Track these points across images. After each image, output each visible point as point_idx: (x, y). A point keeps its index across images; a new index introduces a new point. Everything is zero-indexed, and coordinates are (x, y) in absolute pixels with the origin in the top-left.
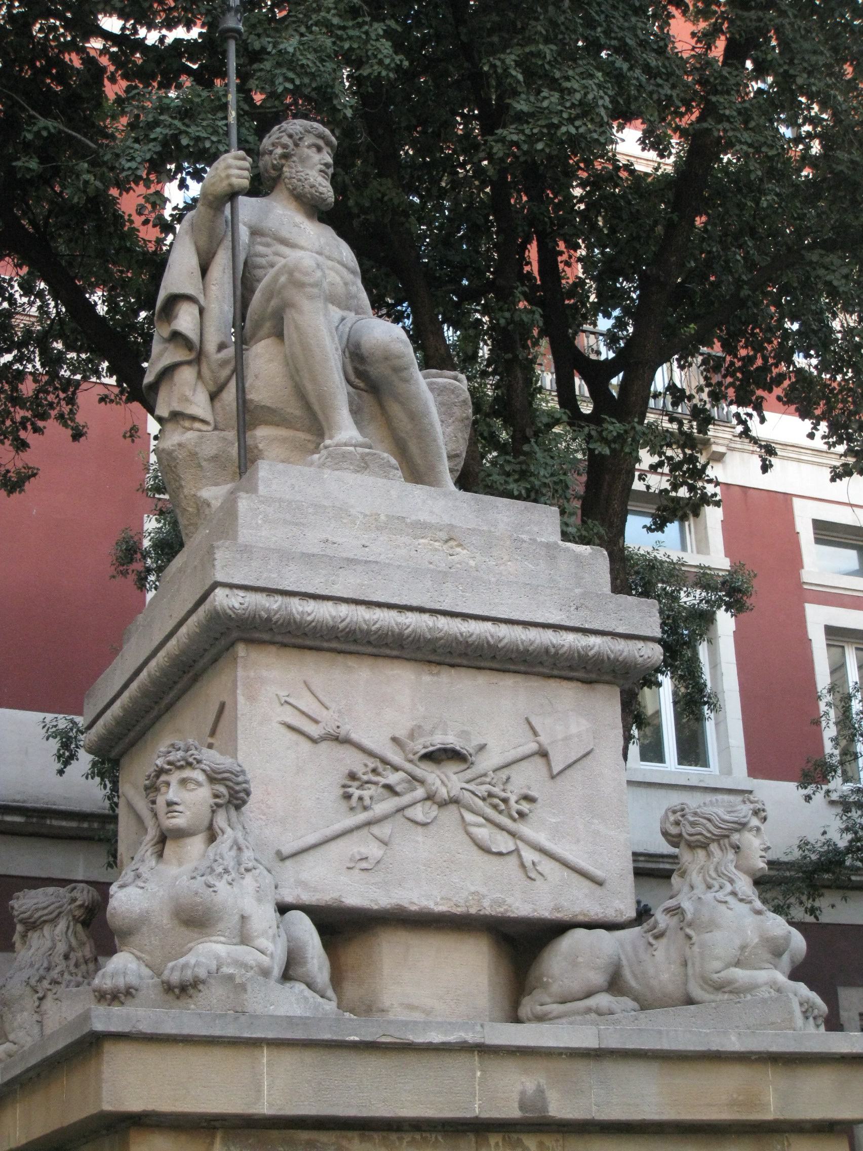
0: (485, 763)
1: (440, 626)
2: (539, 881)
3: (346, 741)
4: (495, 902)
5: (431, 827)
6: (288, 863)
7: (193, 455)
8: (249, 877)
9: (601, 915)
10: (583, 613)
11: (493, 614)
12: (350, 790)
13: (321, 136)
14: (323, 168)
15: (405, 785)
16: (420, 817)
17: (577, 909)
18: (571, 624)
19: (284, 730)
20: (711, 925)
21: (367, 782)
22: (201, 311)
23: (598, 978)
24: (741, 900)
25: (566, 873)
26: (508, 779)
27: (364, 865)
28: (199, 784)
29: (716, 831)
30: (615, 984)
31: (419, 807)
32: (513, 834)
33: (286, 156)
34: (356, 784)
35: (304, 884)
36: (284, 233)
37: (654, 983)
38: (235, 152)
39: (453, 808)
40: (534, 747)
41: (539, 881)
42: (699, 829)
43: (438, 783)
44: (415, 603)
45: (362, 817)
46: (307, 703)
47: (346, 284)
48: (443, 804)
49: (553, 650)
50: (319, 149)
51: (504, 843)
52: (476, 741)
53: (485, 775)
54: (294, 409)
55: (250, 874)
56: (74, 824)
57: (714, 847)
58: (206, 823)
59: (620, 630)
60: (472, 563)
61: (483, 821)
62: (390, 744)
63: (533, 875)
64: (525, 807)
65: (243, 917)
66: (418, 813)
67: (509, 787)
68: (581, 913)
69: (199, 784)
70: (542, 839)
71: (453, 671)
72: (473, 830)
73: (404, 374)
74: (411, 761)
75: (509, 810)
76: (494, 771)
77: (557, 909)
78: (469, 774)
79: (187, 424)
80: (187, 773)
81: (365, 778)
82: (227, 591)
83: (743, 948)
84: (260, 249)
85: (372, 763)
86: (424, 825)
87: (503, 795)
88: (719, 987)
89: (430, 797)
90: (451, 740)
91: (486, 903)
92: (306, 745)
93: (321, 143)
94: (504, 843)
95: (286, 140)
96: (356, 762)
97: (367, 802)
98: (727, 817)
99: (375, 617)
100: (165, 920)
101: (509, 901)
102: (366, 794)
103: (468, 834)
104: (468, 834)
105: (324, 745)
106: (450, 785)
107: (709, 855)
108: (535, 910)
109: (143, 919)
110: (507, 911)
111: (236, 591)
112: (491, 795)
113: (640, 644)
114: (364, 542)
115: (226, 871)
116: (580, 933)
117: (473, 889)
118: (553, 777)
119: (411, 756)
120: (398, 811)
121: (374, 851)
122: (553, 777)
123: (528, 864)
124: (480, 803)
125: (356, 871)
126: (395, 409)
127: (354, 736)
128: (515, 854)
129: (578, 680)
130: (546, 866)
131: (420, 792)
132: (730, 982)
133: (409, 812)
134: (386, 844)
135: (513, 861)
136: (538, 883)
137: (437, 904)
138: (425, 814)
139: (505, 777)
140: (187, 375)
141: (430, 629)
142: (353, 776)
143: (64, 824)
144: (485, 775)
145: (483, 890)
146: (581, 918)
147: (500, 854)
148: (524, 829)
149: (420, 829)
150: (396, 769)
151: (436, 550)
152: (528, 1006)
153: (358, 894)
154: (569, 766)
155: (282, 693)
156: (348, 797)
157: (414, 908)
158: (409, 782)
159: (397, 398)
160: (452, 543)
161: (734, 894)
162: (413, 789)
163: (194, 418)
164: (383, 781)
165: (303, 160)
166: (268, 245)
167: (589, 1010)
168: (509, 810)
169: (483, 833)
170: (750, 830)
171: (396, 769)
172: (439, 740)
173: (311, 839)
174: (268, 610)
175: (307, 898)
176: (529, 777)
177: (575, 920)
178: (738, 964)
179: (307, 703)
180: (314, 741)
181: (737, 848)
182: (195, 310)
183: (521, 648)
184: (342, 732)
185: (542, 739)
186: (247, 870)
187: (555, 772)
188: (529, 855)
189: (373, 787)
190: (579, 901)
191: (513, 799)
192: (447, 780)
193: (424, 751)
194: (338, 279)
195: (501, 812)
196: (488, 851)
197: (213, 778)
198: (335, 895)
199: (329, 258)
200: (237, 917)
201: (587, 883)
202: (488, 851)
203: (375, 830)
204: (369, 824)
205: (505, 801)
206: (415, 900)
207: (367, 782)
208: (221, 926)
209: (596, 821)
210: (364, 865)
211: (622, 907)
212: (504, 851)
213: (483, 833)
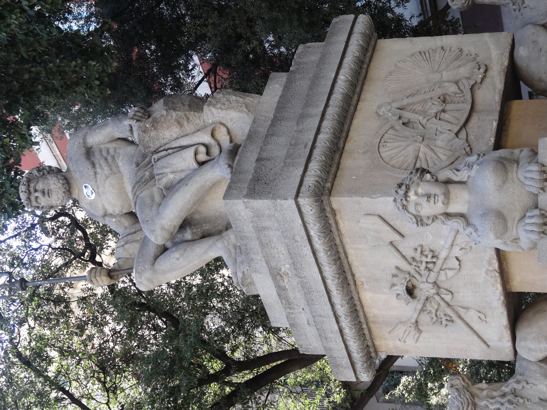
4: (490, 263)
10: (297, 238)
15: (433, 304)
27: (483, 317)
47: (107, 177)
48: (439, 287)
49: (329, 253)
50: (37, 198)
92: (424, 335)
93: (33, 198)
117: (484, 274)
125: (487, 320)
145: (483, 270)
148: (443, 255)
149: (454, 295)
157: (502, 298)
174: (363, 365)
188: (456, 252)
194: (108, 183)
198: (503, 328)
206: (498, 298)
210: (483, 317)
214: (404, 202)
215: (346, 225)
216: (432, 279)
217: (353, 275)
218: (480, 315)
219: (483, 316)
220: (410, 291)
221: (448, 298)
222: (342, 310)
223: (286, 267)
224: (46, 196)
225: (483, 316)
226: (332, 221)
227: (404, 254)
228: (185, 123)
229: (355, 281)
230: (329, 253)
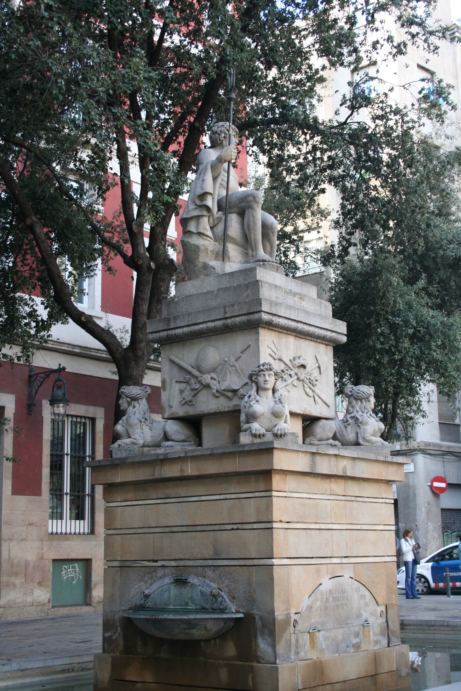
7: (206, 249)
19: (268, 355)
20: (367, 423)
23: (331, 435)
30: (335, 438)
37: (347, 438)
51: (311, 394)
79: (205, 237)
83: (374, 431)
88: (368, 441)
91: (307, 411)
94: (311, 394)
107: (362, 402)
112: (310, 379)
116: (324, 421)
132: (371, 440)
140: (206, 219)
152: (308, 440)
163: (207, 236)
164: (289, 373)
167: (328, 444)
169: (308, 390)
180: (275, 359)
213: (308, 390)
216: (306, 380)
217: (301, 338)
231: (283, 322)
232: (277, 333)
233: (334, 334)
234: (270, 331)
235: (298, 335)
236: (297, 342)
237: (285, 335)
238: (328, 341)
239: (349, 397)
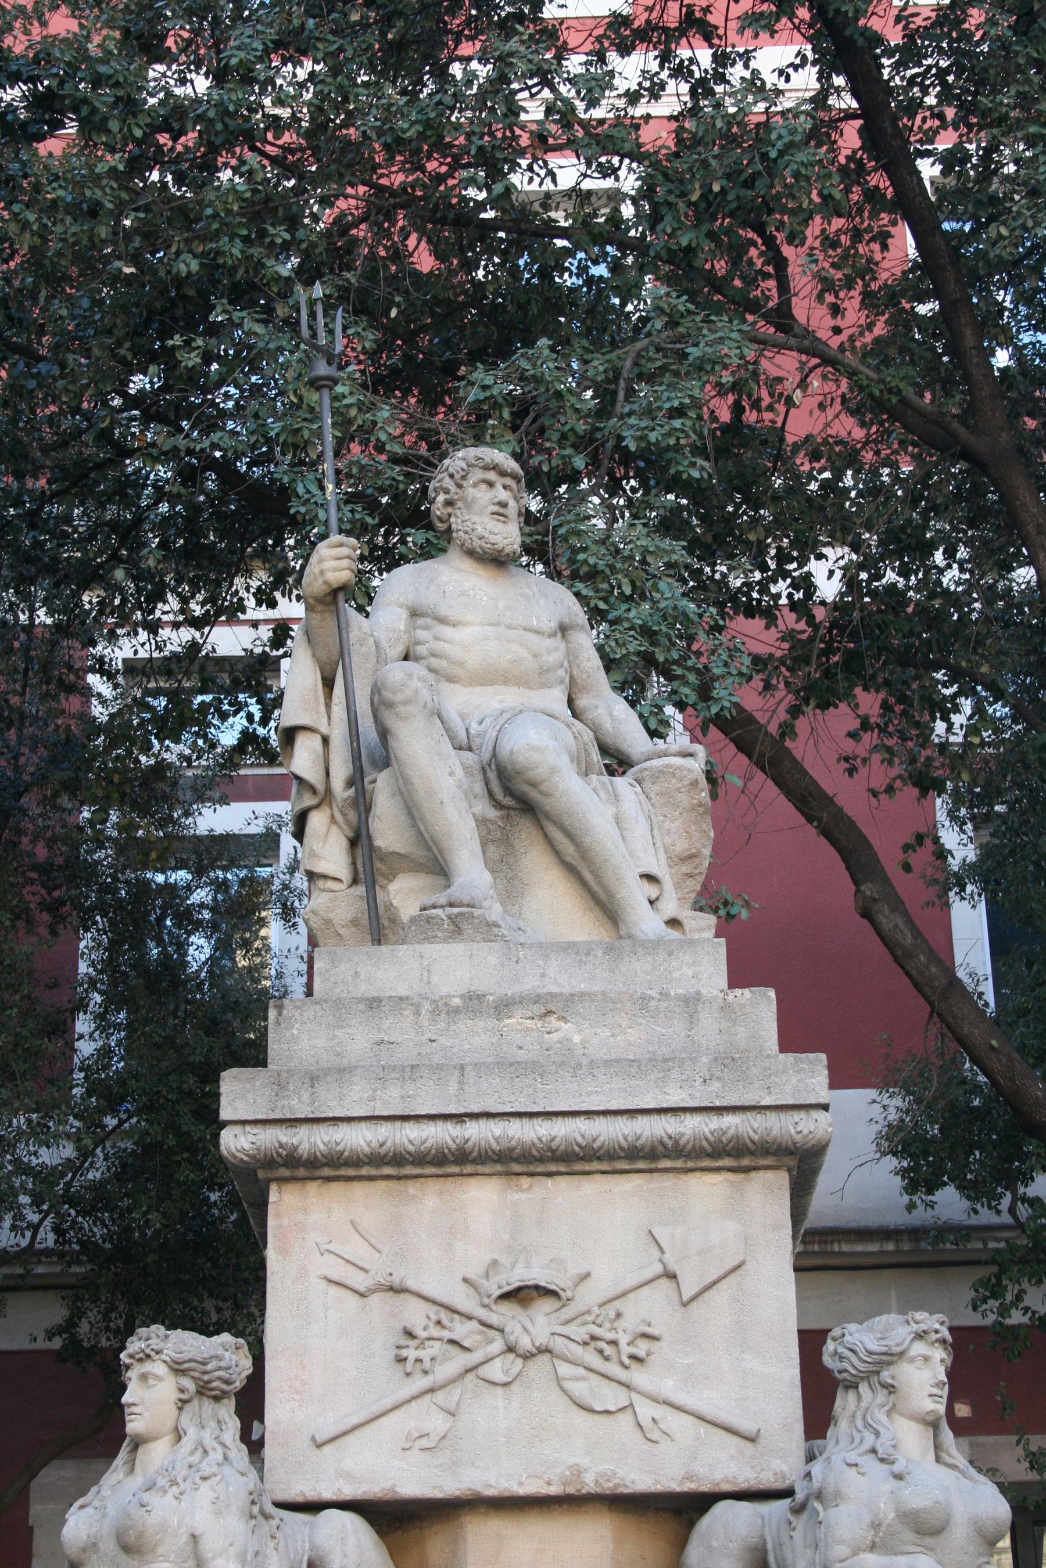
0: (588, 1297)
1: (511, 1133)
2: (664, 1444)
3: (396, 1290)
5: (514, 1387)
6: (326, 1449)
7: (328, 922)
8: (205, 1487)
9: (753, 1482)
10: (716, 1086)
11: (585, 1107)
12: (404, 1353)
13: (495, 467)
14: (496, 508)
16: (499, 1377)
17: (718, 1476)
18: (696, 1104)
19: (324, 1284)
21: (429, 1339)
22: (326, 740)
24: (882, 1460)
25: (703, 1429)
26: (619, 1315)
27: (425, 1443)
28: (159, 1378)
29: (862, 1367)
31: (497, 1363)
32: (628, 1386)
33: (449, 503)
34: (413, 1343)
35: (347, 1475)
36: (443, 611)
38: (335, 538)
39: (546, 1357)
40: (658, 1269)
41: (664, 1444)
42: (845, 1365)
43: (519, 1329)
44: (476, 1109)
45: (425, 1382)
46: (356, 1248)
48: (527, 1356)
50: (491, 484)
52: (575, 1269)
53: (588, 1312)
54: (420, 853)
55: (207, 1483)
56: (873, 1247)
57: (864, 1388)
58: (170, 1424)
59: (767, 1101)
60: (577, 1038)
61: (581, 1371)
62: (463, 1287)
63: (655, 1435)
64: (641, 1348)
65: (194, 1538)
66: (496, 1371)
67: (621, 1324)
68: (726, 1480)
69: (159, 1378)
70: (668, 1387)
71: (549, 1182)
72: (569, 1385)
73: (543, 788)
74: (485, 1306)
75: (618, 1353)
76: (600, 1306)
77: (689, 1478)
78: (567, 1313)
80: (147, 1367)
81: (423, 1334)
82: (237, 1129)
83: (876, 1526)
84: (421, 634)
85: (433, 1311)
86: (506, 1385)
87: (610, 1336)
89: (510, 1349)
90: (536, 1274)
92: (353, 1300)
93: (492, 476)
94: (610, 1397)
95: (448, 483)
96: (416, 1314)
97: (427, 1364)
98: (874, 1347)
99: (424, 1135)
100: (109, 1546)
101: (620, 1472)
102: (425, 1354)
103: (564, 1391)
104: (564, 1391)
105: (376, 1299)
106: (533, 1331)
107: (859, 1398)
108: (657, 1482)
109: (92, 1546)
110: (617, 1485)
111: (248, 1128)
112: (594, 1338)
113: (797, 1116)
114: (429, 1035)
115: (174, 1483)
117: (571, 1461)
118: (685, 1305)
119: (486, 1301)
120: (468, 1371)
121: (438, 1423)
122: (685, 1305)
123: (646, 1422)
124: (578, 1350)
125: (415, 1452)
126: (551, 829)
127: (411, 1284)
128: (630, 1411)
129: (730, 1170)
130: (673, 1421)
131: (498, 1346)
133: (485, 1371)
134: (452, 1414)
135: (626, 1417)
136: (662, 1446)
137: (521, 1484)
138: (506, 1372)
139: (612, 1314)
141: (497, 1140)
142: (409, 1334)
143: (859, 1248)
144: (588, 1312)
145: (584, 1461)
146: (726, 1487)
147: (607, 1412)
148: (639, 1377)
149: (500, 1390)
150: (469, 1318)
151: (527, 1029)
153: (414, 1480)
154: (709, 1287)
155: (322, 1239)
156: (402, 1360)
158: (481, 1333)
159: (549, 818)
160: (552, 1018)
161: (874, 1451)
162: (491, 1341)
164: (447, 1335)
165: (469, 505)
166: (427, 628)
168: (618, 1353)
169: (578, 1389)
170: (912, 1360)
171: (469, 1318)
172: (517, 1277)
173: (355, 1420)
175: (349, 1492)
176: (653, 1307)
177: (716, 1489)
178: (873, 1547)
179: (356, 1248)
181: (890, 1389)
182: (316, 742)
183: (625, 1144)
184: (396, 1280)
185: (667, 1256)
186: (204, 1479)
187: (685, 1298)
188: (645, 1410)
189: (437, 1344)
190: (721, 1465)
191: (623, 1339)
192: (538, 1324)
193: (499, 1292)
194: (523, 653)
195: (607, 1359)
196: (591, 1410)
197: (178, 1369)
198: (387, 1485)
199: (510, 627)
200: (185, 1538)
201: (735, 1439)
202: (591, 1410)
203: (440, 1397)
204: (431, 1390)
205: (614, 1343)
206: (492, 1482)
207: (429, 1339)
208: (160, 1550)
209: (748, 1357)
210: (425, 1443)
211: (785, 1468)
212: (612, 1409)
214: (934, 1337)
215: (707, 1190)
216: (559, 1344)
217: (550, 1175)
218: (434, 1438)
219: (418, 1442)
220: (520, 1295)
221: (496, 1371)
222: (476, 1133)
223: (567, 1031)
224: (496, 508)
225: (418, 1442)
226: (727, 1162)
227: (631, 1296)
228: (685, 868)
229: (532, 1175)
230: (669, 1143)
231: (358, 1138)
232: (382, 1184)
233: (731, 1122)
234: (337, 1187)
235: (516, 1168)
236: (515, 1196)
237: (433, 1185)
238: (752, 1153)
239: (867, 1376)
